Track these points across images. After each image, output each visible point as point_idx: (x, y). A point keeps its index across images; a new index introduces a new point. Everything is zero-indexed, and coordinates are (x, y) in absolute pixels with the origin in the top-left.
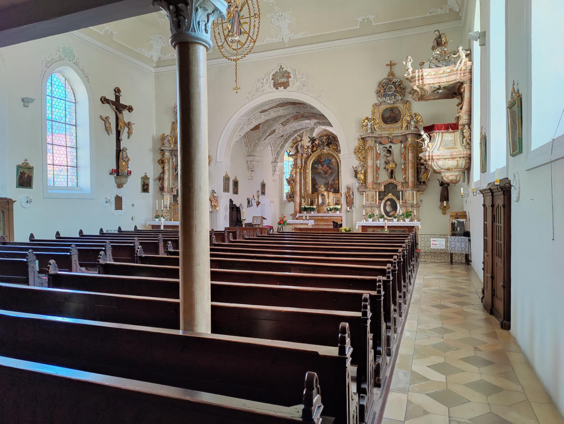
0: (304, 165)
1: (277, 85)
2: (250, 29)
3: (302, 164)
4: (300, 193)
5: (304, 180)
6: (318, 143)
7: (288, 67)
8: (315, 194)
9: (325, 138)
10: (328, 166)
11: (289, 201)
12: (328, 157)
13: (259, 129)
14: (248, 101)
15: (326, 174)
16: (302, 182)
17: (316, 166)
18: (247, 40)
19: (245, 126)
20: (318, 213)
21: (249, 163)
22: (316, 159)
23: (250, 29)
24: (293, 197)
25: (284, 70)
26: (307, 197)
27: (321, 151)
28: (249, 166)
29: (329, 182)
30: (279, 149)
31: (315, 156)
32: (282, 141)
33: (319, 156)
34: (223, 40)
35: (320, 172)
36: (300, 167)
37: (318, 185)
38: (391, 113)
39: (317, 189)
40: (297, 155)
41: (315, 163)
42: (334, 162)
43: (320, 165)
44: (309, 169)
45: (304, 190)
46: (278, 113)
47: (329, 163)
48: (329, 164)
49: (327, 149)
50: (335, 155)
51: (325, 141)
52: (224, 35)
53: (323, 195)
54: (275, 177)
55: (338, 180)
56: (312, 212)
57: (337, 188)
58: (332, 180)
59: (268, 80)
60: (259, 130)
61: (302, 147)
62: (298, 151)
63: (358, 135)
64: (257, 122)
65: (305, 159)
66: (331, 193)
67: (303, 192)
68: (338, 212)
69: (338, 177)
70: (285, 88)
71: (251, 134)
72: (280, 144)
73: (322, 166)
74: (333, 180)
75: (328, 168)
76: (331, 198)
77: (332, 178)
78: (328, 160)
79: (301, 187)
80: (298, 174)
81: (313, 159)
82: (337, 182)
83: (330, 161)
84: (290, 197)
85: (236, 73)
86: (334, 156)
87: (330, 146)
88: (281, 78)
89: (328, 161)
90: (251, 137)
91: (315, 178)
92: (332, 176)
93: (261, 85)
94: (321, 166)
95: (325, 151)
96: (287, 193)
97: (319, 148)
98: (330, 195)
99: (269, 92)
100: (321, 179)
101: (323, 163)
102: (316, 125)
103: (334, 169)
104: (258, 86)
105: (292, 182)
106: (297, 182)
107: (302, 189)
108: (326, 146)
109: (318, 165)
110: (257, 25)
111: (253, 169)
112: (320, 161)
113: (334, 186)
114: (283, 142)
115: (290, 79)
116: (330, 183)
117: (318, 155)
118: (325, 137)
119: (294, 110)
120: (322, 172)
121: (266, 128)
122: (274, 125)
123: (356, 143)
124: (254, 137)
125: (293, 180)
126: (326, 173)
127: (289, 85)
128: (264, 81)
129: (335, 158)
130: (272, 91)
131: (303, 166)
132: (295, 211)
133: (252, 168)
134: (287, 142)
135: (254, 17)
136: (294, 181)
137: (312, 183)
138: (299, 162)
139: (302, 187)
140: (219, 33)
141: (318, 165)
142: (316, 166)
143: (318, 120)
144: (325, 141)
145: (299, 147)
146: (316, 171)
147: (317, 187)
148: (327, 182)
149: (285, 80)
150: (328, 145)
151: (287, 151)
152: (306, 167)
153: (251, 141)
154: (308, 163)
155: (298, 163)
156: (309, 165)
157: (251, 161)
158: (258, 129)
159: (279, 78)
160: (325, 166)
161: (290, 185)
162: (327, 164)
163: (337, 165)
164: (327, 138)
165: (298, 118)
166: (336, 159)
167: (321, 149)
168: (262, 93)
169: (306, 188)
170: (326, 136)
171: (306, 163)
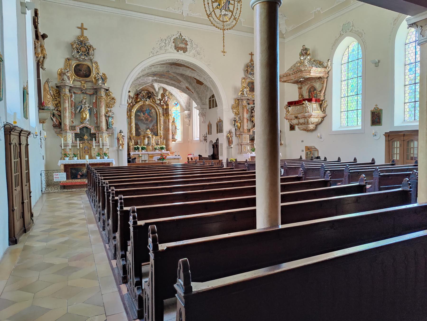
1: (178, 49)
7: (186, 37)
10: (149, 115)
12: (149, 108)
14: (153, 55)
17: (139, 113)
18: (231, 17)
25: (183, 38)
27: (144, 102)
29: (149, 127)
33: (141, 106)
34: (211, 10)
35: (142, 119)
37: (141, 129)
38: (252, 85)
39: (140, 132)
41: (137, 111)
42: (154, 112)
43: (142, 113)
47: (149, 112)
51: (145, 95)
52: (212, 6)
53: (148, 137)
55: (157, 125)
57: (156, 132)
59: (170, 42)
63: (235, 97)
69: (156, 123)
70: (184, 52)
73: (144, 114)
74: (153, 125)
75: (148, 116)
76: (153, 140)
77: (152, 124)
81: (137, 108)
82: (156, 128)
85: (224, 40)
86: (153, 107)
88: (180, 43)
89: (149, 111)
91: (138, 124)
93: (163, 44)
94: (143, 114)
97: (143, 100)
99: (171, 52)
100: (143, 124)
101: (145, 112)
102: (153, 82)
103: (154, 117)
104: (161, 45)
109: (140, 113)
112: (142, 110)
113: (154, 130)
115: (187, 46)
117: (140, 105)
118: (146, 92)
120: (143, 119)
123: (232, 102)
126: (147, 120)
127: (187, 51)
128: (167, 42)
130: (174, 52)
140: (208, 3)
141: (140, 113)
142: (139, 113)
143: (159, 78)
144: (145, 95)
146: (139, 118)
147: (140, 131)
148: (148, 127)
149: (184, 46)
150: (149, 97)
154: (132, 110)
156: (134, 113)
159: (178, 43)
160: (146, 114)
164: (147, 93)
166: (155, 109)
167: (144, 100)
168: (166, 51)
170: (146, 90)
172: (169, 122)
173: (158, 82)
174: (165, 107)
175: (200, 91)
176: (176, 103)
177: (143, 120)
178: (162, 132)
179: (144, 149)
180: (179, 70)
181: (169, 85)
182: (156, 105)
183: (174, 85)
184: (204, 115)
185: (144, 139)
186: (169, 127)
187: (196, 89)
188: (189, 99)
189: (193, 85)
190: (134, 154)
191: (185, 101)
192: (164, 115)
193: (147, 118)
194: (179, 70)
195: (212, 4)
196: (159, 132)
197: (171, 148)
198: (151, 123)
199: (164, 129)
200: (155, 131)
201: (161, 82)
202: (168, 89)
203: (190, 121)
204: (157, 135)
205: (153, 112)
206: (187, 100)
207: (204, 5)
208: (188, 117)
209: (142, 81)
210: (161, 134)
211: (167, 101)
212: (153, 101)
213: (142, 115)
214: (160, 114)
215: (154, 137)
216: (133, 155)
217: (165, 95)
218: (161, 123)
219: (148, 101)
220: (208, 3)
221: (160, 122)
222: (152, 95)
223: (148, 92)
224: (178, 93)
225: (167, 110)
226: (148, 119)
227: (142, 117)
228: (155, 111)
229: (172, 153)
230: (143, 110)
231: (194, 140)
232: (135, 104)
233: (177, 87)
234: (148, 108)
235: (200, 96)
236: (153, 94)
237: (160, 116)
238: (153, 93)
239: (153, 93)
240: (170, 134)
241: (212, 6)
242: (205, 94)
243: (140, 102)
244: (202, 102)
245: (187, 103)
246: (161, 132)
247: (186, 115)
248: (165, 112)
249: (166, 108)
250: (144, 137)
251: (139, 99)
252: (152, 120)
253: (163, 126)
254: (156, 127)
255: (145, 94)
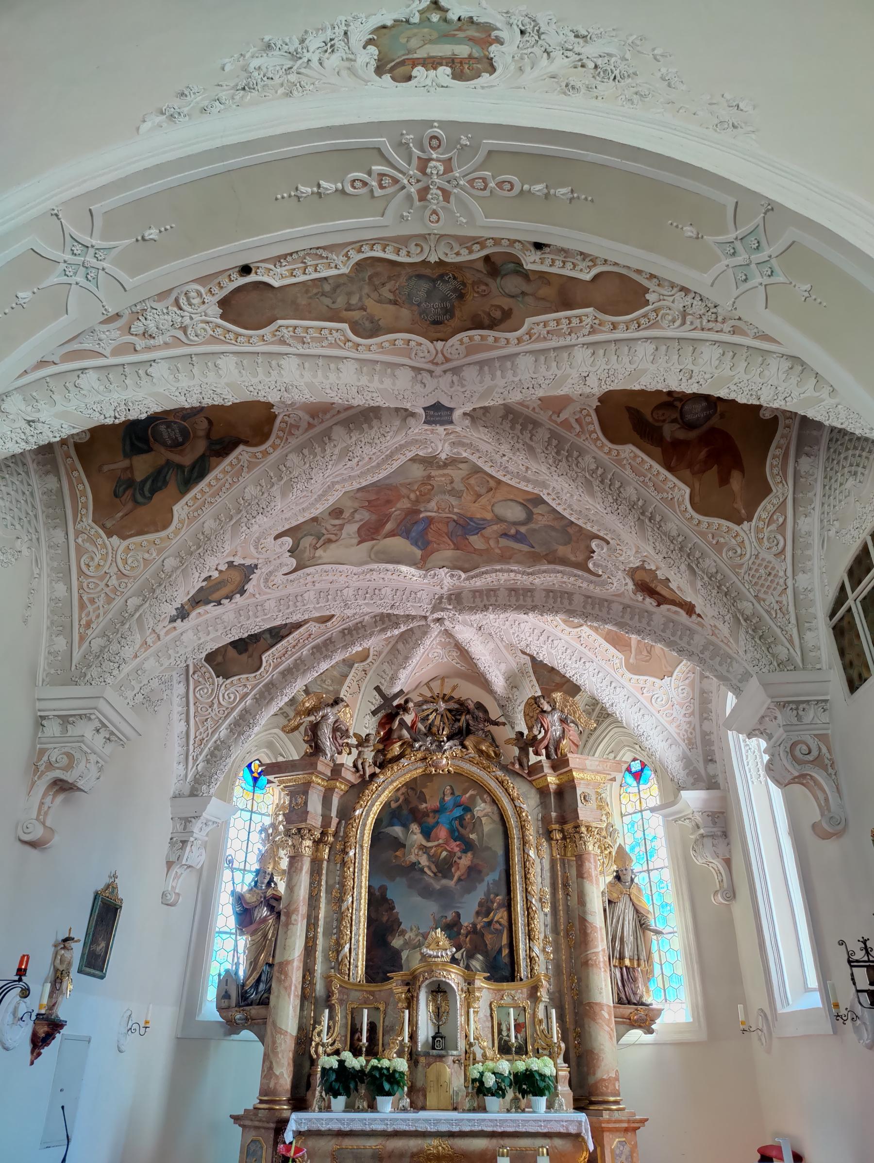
0: (339, 823)
3: (326, 821)
4: (304, 977)
5: (328, 903)
6: (414, 723)
8: (396, 987)
9: (442, 706)
10: (455, 835)
11: (232, 1027)
12: (457, 793)
13: (165, 527)
15: (445, 877)
16: (322, 915)
17: (397, 830)
19: (92, 375)
20: (415, 1106)
21: (53, 729)
22: (397, 800)
24: (264, 1002)
26: (341, 1002)
28: (42, 752)
29: (458, 915)
30: (223, 732)
31: (393, 781)
32: (246, 695)
33: (411, 786)
35: (414, 864)
36: (317, 834)
37: (403, 933)
40: (314, 766)
42: (486, 815)
43: (414, 827)
44: (362, 847)
45: (326, 959)
46: (327, 377)
47: (461, 818)
48: (462, 826)
49: (457, 750)
50: (493, 785)
51: (437, 722)
53: (440, 990)
54: (177, 877)
55: (509, 905)
56: (386, 1104)
57: (505, 952)
58: (476, 907)
60: (163, 534)
61: (338, 734)
62: (317, 749)
64: (184, 383)
65: (342, 797)
66: (480, 982)
67: (319, 968)
68: (542, 1102)
71: (104, 557)
72: (233, 709)
73: (427, 833)
74: (481, 904)
75: (455, 846)
77: (479, 894)
78: (458, 805)
79: (315, 938)
80: (306, 866)
81: (384, 798)
82: (504, 921)
83: (468, 809)
84: (244, 999)
86: (483, 789)
87: (467, 743)
89: (458, 812)
90: (102, 578)
91: (389, 895)
92: (474, 888)
94: (422, 832)
95: (444, 761)
96: (227, 979)
97: (417, 745)
98: (480, 989)
100: (419, 899)
101: (431, 820)
102: (443, 610)
103: (488, 848)
105: (265, 912)
106: (296, 910)
107: (319, 955)
108: (449, 738)
109: (406, 826)
111: (69, 767)
112: (417, 806)
113: (489, 938)
114: (249, 701)
116: (466, 922)
117: (408, 777)
119: (418, 387)
120: (424, 861)
121: (210, 524)
122: (263, 504)
124: (121, 574)
125: (273, 903)
126: (444, 868)
129: (488, 799)
131: (332, 829)
132: (264, 1091)
133: (65, 761)
134: (272, 699)
136: (271, 908)
137: (370, 921)
138: (315, 805)
139: (320, 941)
141: (406, 826)
142: (397, 830)
143: (463, 575)
145: (326, 733)
146: (396, 856)
147: (397, 942)
148: (450, 916)
150: (460, 735)
151: (249, 766)
152: (346, 835)
153: (100, 602)
154: (357, 813)
155: (310, 808)
156: (364, 825)
157: (65, 720)
158: (157, 531)
160: (442, 833)
161: (253, 927)
162: (450, 823)
163: (500, 828)
164: (450, 711)
165: (381, 524)
166: (494, 802)
167: (427, 749)
169: (338, 947)
170: (446, 699)
171: (346, 814)
172: (582, 878)
173: (473, 609)
174: (552, 780)
175: (737, 574)
176: (633, 770)
177: (422, 870)
178: (544, 950)
179: (387, 1086)
180: (510, 373)
181: (533, 608)
182: (500, 774)
183: (566, 602)
184: (818, 762)
185: (411, 1003)
186: (585, 912)
187: (703, 555)
188: (701, 714)
189: (672, 526)
190: (304, 1128)
191: (672, 729)
192: (548, 835)
193: (444, 853)
194: (510, 373)
196: (522, 954)
197: (617, 1079)
198: (469, 890)
199: (555, 930)
200: (497, 947)
201: (486, 602)
202: (549, 653)
203: (728, 862)
204: (506, 973)
205: (484, 820)
206: (690, 723)
208: (713, 836)
209: (361, 602)
210: (541, 968)
211: (557, 743)
212: (480, 752)
213: (415, 837)
214: (522, 828)
215: (484, 989)
216: (298, 1134)
217: (546, 707)
218: (534, 889)
219: (447, 754)
221: (526, 877)
222: (475, 718)
223: (456, 706)
224: (619, 678)
225: (568, 797)
226: (451, 866)
227: (415, 850)
228: (496, 808)
229: (626, 1130)
230: (424, 805)
231: (780, 1010)
232: (373, 776)
233: (584, 607)
234: (453, 793)
235: (746, 606)
236: (481, 715)
237: (524, 842)
238: (480, 706)
239: (486, 711)
240: (596, 965)
242: (790, 591)
243: (403, 760)
244: (773, 655)
245: (691, 744)
246: (537, 950)
247: (698, 818)
248: (554, 814)
249: (558, 785)
250: (411, 984)
251: (399, 743)
252: (480, 872)
253: (547, 910)
254: (501, 916)
255: (439, 718)
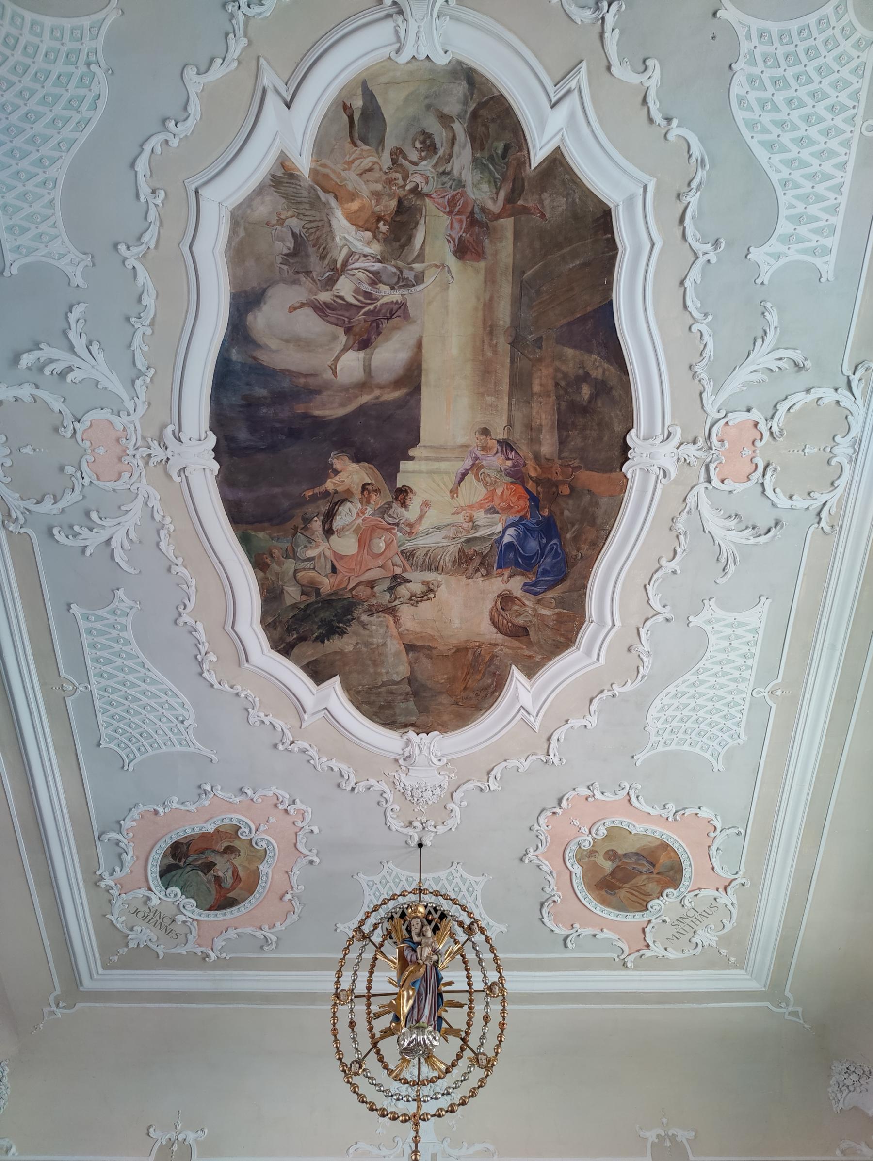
2: (469, 1025)
23: (469, 1025)
34: (365, 1044)
52: (371, 1029)
110: (495, 1018)
135: (484, 994)
140: (352, 1024)
195: (370, 1023)
207: (335, 1032)
220: (352, 1024)
241: (371, 1029)
